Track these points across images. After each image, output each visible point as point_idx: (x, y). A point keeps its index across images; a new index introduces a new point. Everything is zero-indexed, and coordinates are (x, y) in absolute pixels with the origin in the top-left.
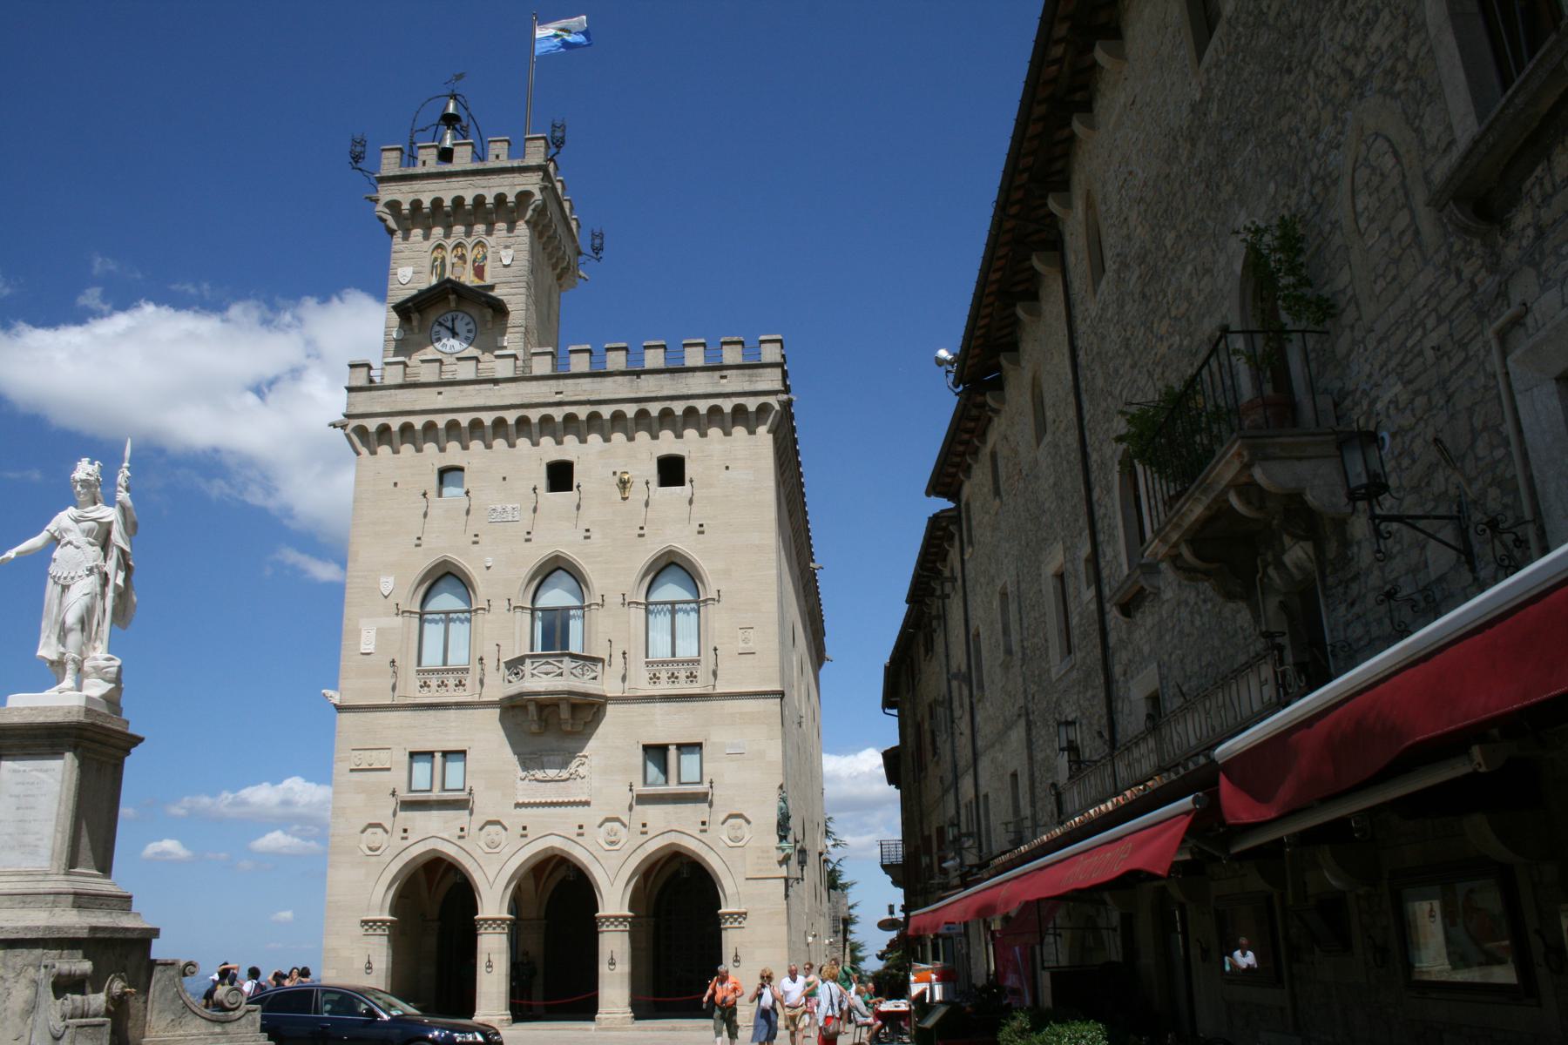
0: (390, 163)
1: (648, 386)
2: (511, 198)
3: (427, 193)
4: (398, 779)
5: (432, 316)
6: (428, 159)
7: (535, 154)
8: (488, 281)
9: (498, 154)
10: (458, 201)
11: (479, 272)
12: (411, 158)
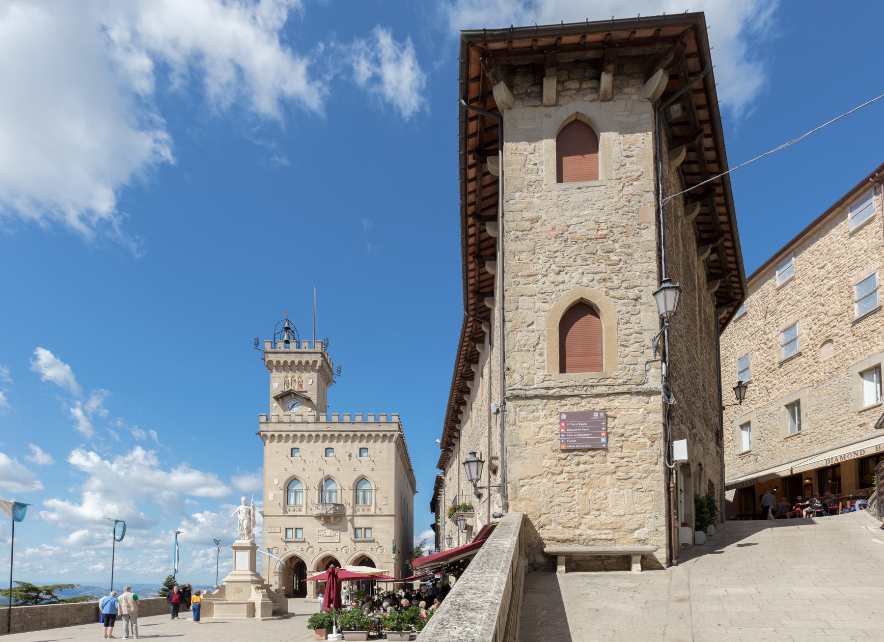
0: (268, 347)
1: (357, 427)
2: (311, 363)
3: (282, 358)
4: (283, 535)
5: (286, 399)
6: (281, 345)
7: (318, 348)
8: (304, 389)
9: (305, 346)
10: (293, 362)
11: (301, 386)
12: (274, 344)
